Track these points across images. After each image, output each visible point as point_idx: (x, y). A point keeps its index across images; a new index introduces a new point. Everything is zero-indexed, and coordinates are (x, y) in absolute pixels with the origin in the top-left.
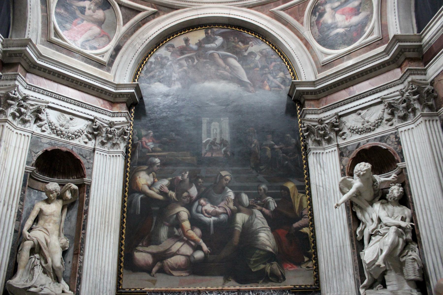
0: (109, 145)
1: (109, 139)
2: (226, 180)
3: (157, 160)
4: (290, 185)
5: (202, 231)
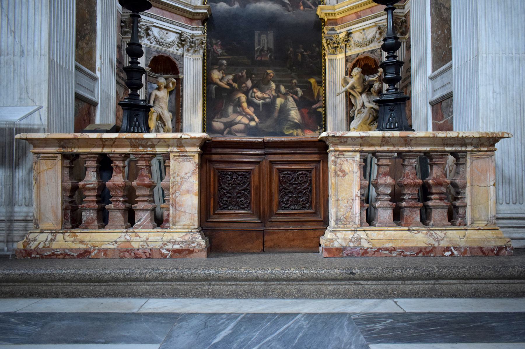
0: (191, 51)
1: (191, 47)
2: (271, 76)
3: (225, 62)
4: (312, 81)
5: (255, 109)
